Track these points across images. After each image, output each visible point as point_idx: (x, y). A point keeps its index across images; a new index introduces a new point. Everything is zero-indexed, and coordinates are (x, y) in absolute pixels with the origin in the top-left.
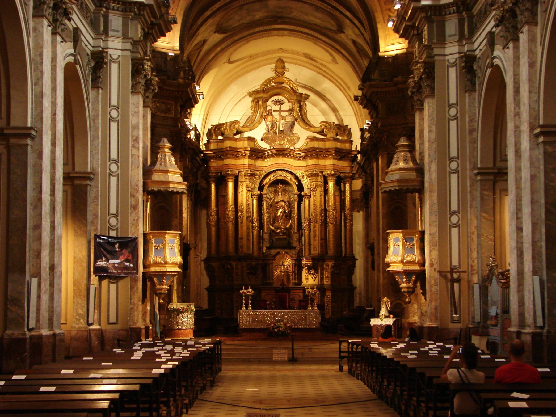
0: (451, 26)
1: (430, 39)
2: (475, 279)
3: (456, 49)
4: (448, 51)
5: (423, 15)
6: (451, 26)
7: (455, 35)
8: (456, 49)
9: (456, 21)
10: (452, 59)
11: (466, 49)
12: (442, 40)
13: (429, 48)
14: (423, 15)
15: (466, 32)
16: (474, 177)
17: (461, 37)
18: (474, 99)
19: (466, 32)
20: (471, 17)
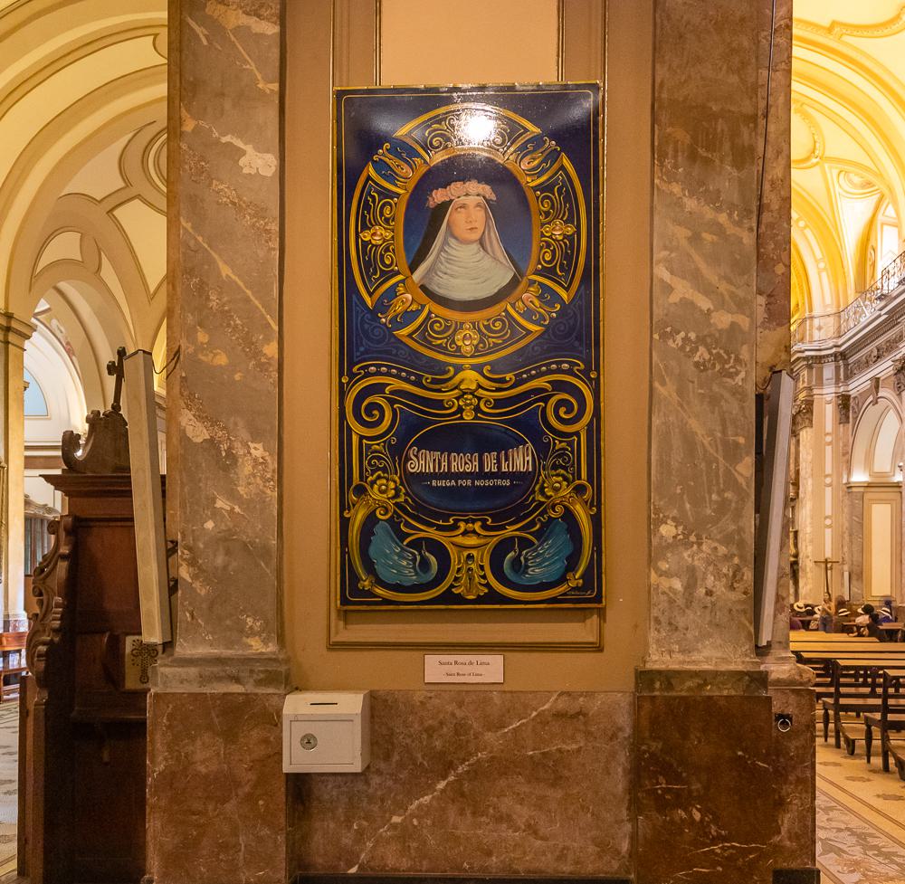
0: (829, 371)
1: (809, 382)
2: (846, 567)
3: (833, 390)
4: (825, 391)
5: (805, 363)
6: (829, 371)
7: (832, 379)
8: (833, 390)
9: (834, 367)
10: (829, 398)
11: (842, 389)
12: (820, 383)
13: (810, 389)
14: (805, 363)
15: (842, 377)
16: (846, 489)
17: (838, 380)
18: (848, 428)
19: (842, 377)
20: (846, 365)
